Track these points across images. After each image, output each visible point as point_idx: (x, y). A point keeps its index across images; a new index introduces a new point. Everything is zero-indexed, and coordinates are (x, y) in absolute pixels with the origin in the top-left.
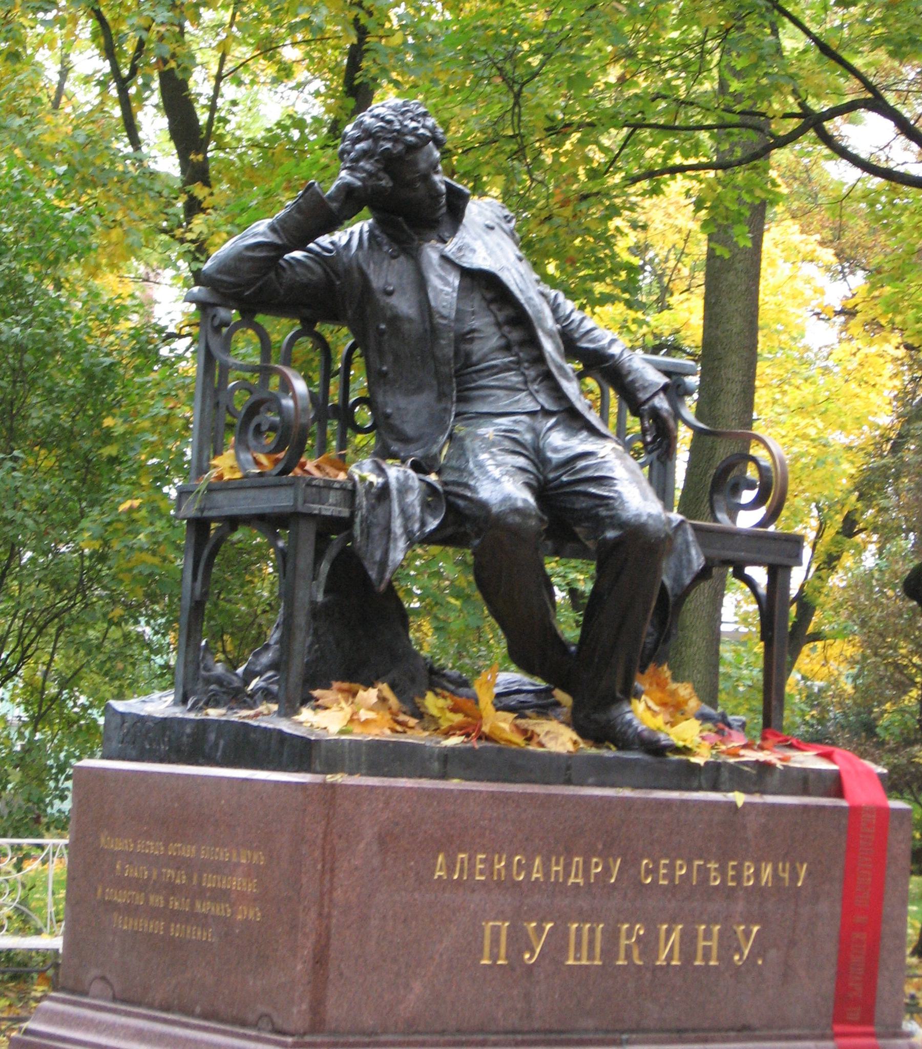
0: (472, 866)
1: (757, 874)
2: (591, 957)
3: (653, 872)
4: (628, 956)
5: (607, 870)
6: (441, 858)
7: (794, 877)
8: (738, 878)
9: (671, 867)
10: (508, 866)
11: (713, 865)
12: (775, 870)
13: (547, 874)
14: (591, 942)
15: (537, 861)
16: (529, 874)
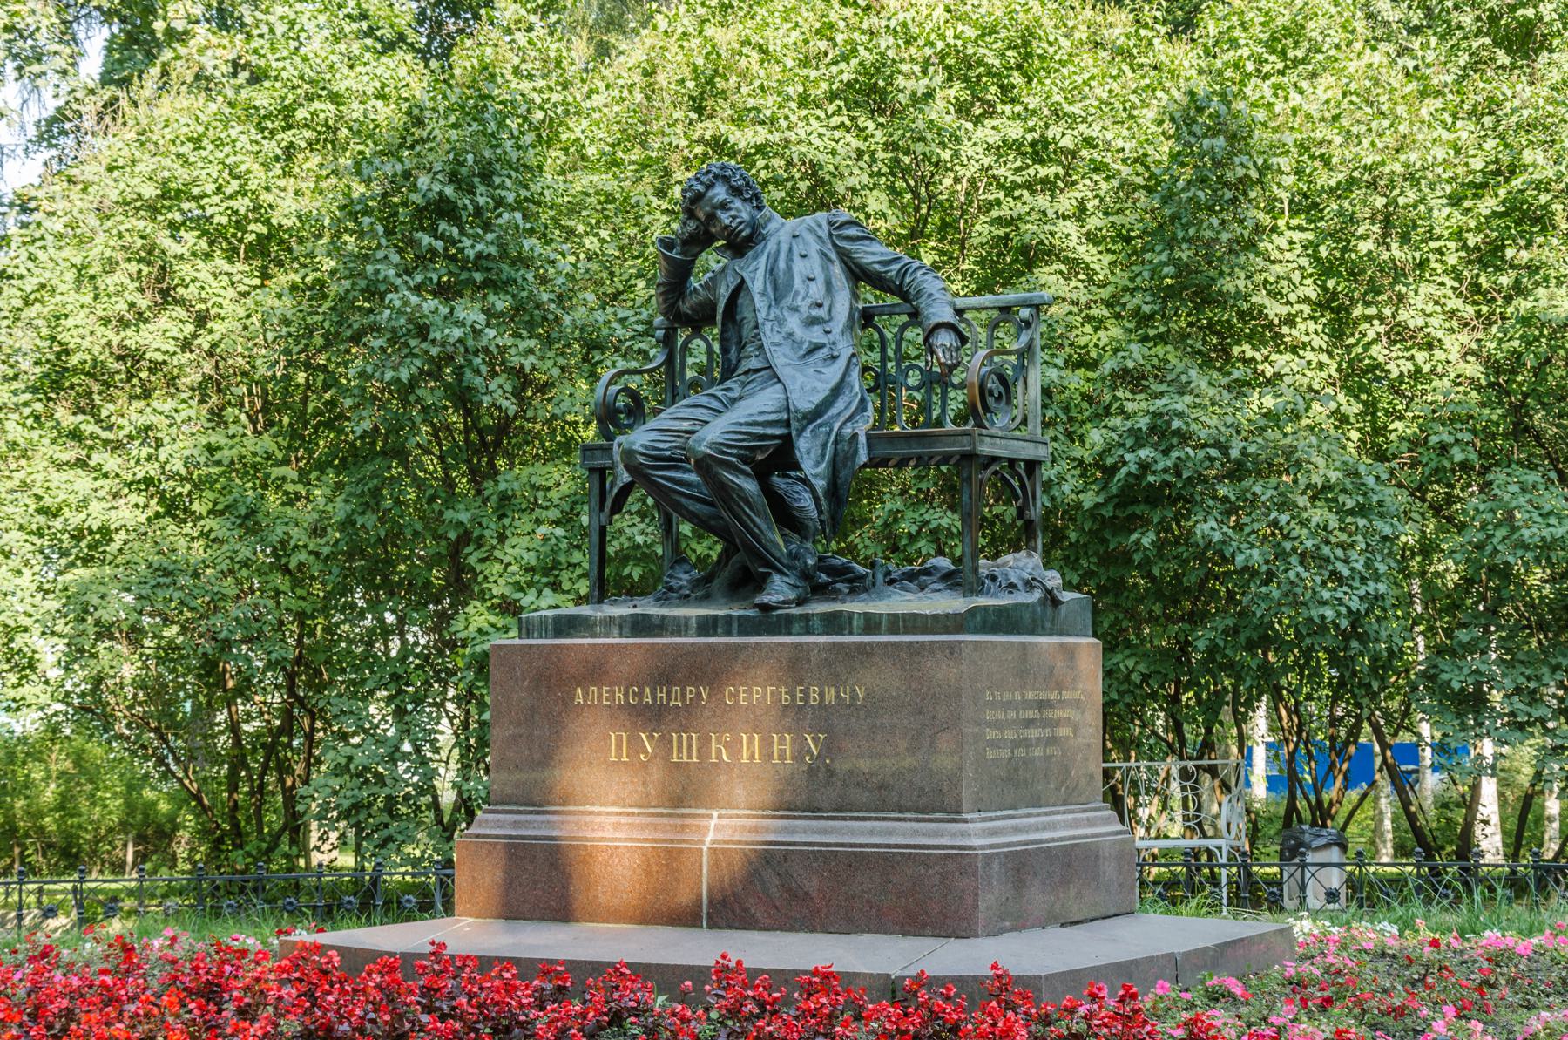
0: (600, 695)
1: (822, 695)
2: (690, 757)
3: (735, 695)
4: (719, 756)
5: (699, 694)
6: (579, 690)
7: (854, 697)
8: (806, 698)
9: (749, 692)
10: (626, 695)
11: (783, 690)
12: (838, 692)
13: (654, 699)
14: (690, 747)
15: (648, 690)
16: (641, 699)
